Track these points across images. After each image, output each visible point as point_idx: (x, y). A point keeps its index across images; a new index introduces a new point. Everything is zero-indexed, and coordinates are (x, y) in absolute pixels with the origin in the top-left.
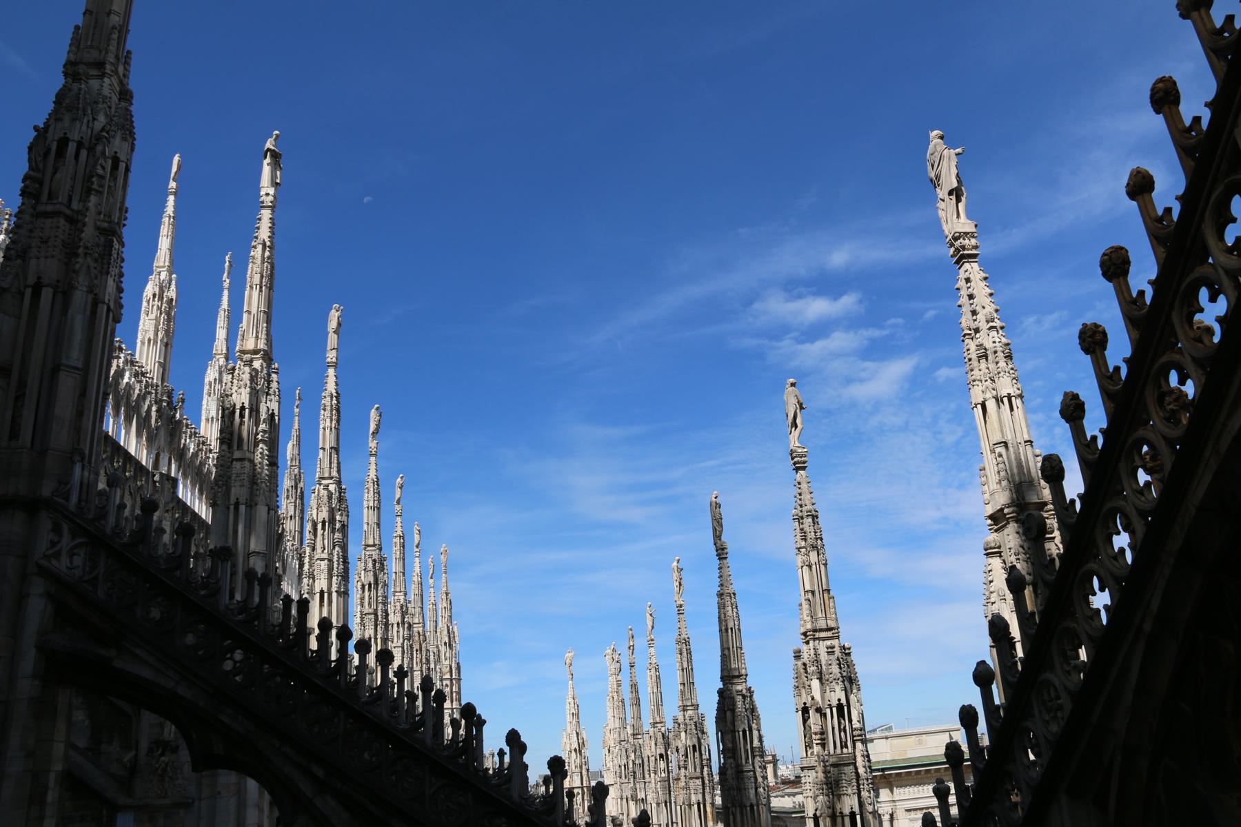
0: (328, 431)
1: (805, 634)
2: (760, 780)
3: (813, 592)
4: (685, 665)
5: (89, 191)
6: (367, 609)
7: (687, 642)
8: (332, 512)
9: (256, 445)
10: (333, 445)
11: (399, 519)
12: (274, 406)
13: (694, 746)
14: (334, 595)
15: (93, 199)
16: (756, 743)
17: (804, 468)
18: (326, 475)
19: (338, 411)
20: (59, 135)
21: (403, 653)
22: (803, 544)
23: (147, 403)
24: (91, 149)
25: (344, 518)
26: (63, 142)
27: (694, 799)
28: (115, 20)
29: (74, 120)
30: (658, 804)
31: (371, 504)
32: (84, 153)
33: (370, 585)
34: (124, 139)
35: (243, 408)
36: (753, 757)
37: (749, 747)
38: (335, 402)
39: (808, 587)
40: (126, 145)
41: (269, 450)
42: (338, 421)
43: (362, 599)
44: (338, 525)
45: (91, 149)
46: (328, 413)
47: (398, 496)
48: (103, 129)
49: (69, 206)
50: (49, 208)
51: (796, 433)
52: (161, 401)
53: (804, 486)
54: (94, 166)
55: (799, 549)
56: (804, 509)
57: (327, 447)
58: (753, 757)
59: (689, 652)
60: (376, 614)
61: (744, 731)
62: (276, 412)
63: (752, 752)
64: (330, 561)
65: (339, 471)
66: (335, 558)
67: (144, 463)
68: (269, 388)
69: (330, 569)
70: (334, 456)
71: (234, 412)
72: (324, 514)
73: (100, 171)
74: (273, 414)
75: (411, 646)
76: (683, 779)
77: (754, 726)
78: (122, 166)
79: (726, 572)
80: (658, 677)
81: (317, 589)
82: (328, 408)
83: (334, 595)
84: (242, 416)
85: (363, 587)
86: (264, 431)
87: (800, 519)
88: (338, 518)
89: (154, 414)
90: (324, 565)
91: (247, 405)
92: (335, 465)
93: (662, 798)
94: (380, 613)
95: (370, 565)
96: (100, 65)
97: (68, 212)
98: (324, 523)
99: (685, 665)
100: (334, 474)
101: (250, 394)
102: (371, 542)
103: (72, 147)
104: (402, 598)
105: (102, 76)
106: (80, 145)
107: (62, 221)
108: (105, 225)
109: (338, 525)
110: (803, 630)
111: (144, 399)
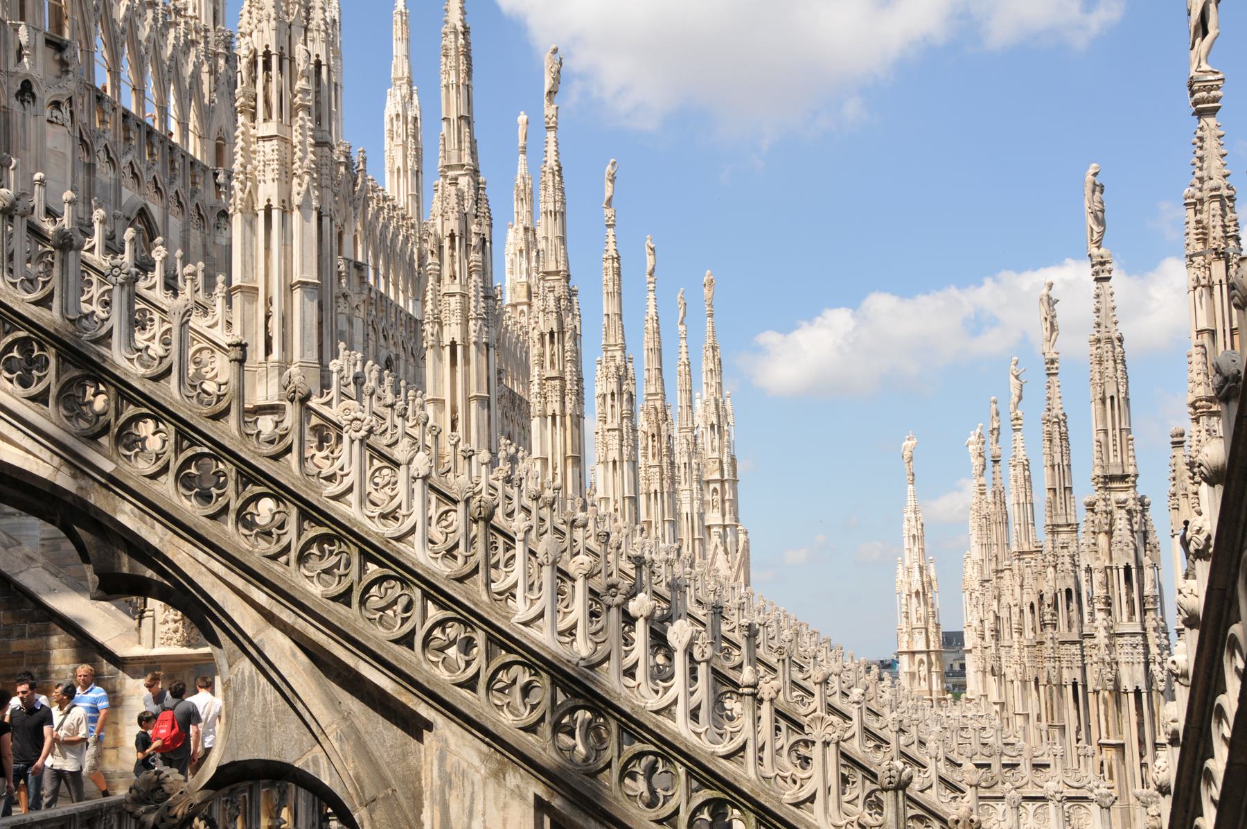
0: (453, 92)
1: (1193, 405)
2: (1154, 650)
3: (1213, 333)
4: (1057, 460)
6: (550, 373)
7: (1062, 421)
8: (464, 218)
9: (293, 113)
10: (463, 112)
11: (610, 231)
12: (318, 49)
13: (1068, 591)
14: (473, 348)
16: (1148, 590)
17: (1213, 112)
18: (454, 162)
19: (468, 56)
21: (622, 439)
22: (1199, 247)
23: (192, 58)
25: (485, 230)
27: (1067, 676)
30: (1024, 683)
31: (551, 207)
33: (552, 334)
35: (267, 55)
36: (1144, 612)
37: (1135, 595)
38: (461, 41)
39: (1203, 325)
41: (318, 120)
42: (469, 72)
43: (542, 355)
44: (474, 241)
46: (452, 61)
47: (608, 194)
51: (1202, 45)
52: (216, 55)
53: (1211, 143)
55: (1190, 257)
56: (1208, 185)
57: (453, 116)
58: (1144, 612)
59: (1064, 438)
60: (562, 379)
61: (1127, 569)
62: (323, 60)
63: (1142, 604)
64: (463, 296)
65: (473, 153)
66: (472, 293)
67: (198, 157)
68: (308, 19)
69: (465, 310)
70: (465, 130)
71: (253, 63)
72: (453, 224)
74: (318, 65)
75: (635, 430)
76: (1049, 644)
77: (1146, 561)
79: (1106, 302)
80: (1028, 479)
81: (447, 341)
82: (452, 53)
83: (473, 348)
84: (267, 67)
85: (542, 335)
86: (305, 91)
87: (1196, 204)
88: (474, 228)
89: (205, 77)
90: (454, 302)
91: (273, 49)
92: (466, 145)
93: (1030, 674)
94: (568, 377)
95: (552, 303)
98: (452, 236)
99: (1057, 460)
100: (467, 159)
101: (277, 30)
102: (552, 267)
104: (618, 354)
109: (474, 241)
110: (1191, 399)
111: (186, 53)
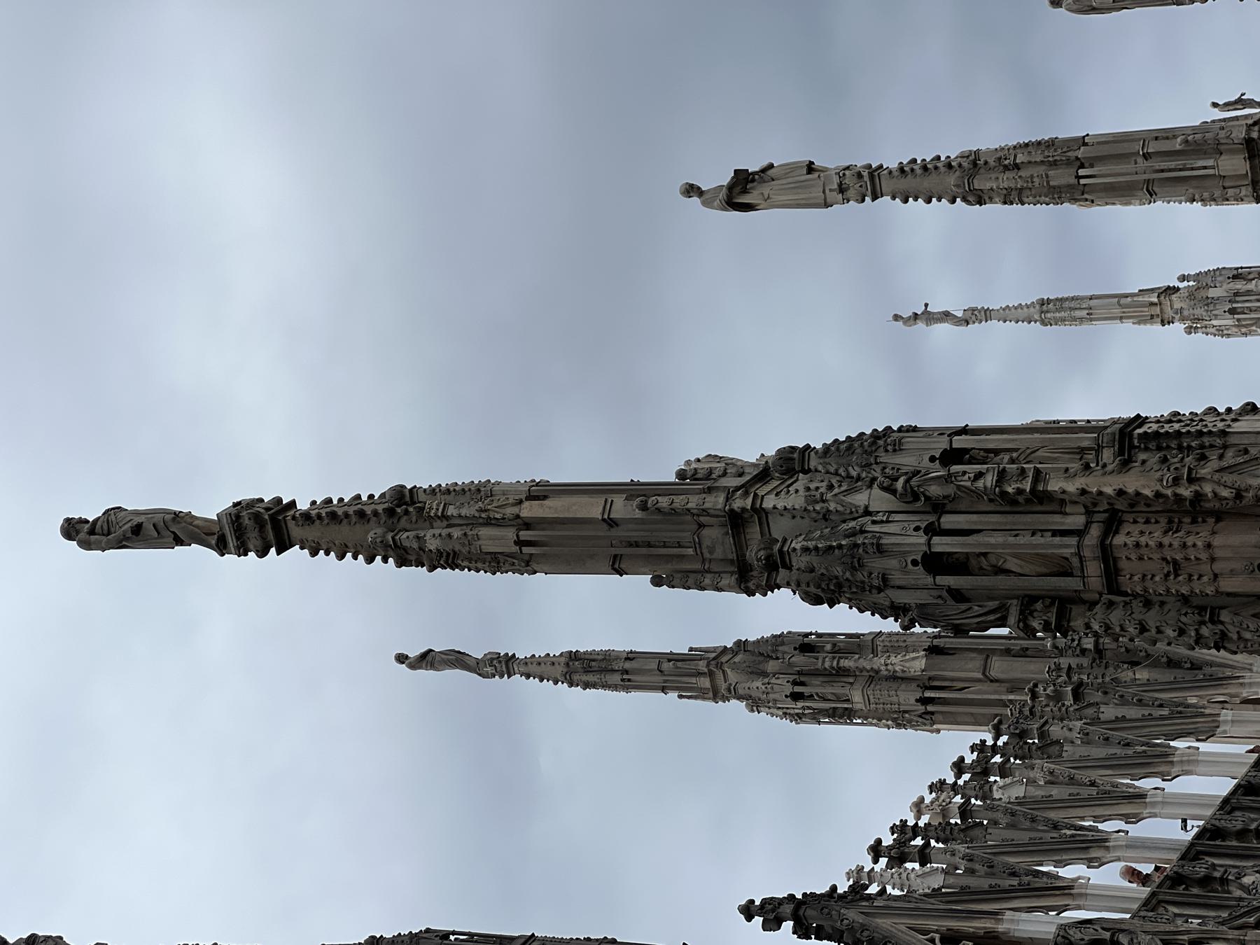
5: (1041, 499)
15: (1054, 485)
20: (921, 576)
24: (938, 507)
26: (934, 563)
28: (621, 508)
29: (880, 549)
32: (948, 521)
34: (897, 448)
40: (910, 441)
45: (938, 507)
48: (890, 490)
49: (1080, 533)
50: (1094, 569)
54: (977, 494)
73: (989, 480)
78: (960, 442)
96: (736, 521)
97: (1095, 531)
103: (942, 544)
105: (760, 513)
106: (932, 530)
107: (1119, 540)
108: (1107, 455)
